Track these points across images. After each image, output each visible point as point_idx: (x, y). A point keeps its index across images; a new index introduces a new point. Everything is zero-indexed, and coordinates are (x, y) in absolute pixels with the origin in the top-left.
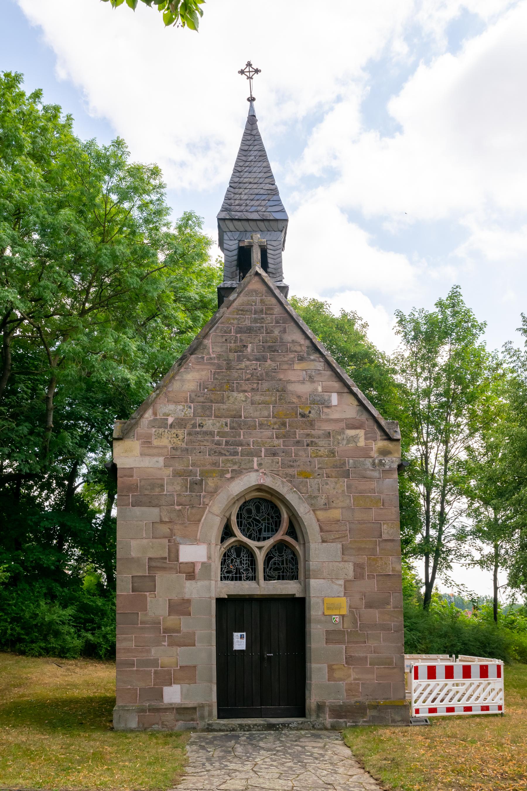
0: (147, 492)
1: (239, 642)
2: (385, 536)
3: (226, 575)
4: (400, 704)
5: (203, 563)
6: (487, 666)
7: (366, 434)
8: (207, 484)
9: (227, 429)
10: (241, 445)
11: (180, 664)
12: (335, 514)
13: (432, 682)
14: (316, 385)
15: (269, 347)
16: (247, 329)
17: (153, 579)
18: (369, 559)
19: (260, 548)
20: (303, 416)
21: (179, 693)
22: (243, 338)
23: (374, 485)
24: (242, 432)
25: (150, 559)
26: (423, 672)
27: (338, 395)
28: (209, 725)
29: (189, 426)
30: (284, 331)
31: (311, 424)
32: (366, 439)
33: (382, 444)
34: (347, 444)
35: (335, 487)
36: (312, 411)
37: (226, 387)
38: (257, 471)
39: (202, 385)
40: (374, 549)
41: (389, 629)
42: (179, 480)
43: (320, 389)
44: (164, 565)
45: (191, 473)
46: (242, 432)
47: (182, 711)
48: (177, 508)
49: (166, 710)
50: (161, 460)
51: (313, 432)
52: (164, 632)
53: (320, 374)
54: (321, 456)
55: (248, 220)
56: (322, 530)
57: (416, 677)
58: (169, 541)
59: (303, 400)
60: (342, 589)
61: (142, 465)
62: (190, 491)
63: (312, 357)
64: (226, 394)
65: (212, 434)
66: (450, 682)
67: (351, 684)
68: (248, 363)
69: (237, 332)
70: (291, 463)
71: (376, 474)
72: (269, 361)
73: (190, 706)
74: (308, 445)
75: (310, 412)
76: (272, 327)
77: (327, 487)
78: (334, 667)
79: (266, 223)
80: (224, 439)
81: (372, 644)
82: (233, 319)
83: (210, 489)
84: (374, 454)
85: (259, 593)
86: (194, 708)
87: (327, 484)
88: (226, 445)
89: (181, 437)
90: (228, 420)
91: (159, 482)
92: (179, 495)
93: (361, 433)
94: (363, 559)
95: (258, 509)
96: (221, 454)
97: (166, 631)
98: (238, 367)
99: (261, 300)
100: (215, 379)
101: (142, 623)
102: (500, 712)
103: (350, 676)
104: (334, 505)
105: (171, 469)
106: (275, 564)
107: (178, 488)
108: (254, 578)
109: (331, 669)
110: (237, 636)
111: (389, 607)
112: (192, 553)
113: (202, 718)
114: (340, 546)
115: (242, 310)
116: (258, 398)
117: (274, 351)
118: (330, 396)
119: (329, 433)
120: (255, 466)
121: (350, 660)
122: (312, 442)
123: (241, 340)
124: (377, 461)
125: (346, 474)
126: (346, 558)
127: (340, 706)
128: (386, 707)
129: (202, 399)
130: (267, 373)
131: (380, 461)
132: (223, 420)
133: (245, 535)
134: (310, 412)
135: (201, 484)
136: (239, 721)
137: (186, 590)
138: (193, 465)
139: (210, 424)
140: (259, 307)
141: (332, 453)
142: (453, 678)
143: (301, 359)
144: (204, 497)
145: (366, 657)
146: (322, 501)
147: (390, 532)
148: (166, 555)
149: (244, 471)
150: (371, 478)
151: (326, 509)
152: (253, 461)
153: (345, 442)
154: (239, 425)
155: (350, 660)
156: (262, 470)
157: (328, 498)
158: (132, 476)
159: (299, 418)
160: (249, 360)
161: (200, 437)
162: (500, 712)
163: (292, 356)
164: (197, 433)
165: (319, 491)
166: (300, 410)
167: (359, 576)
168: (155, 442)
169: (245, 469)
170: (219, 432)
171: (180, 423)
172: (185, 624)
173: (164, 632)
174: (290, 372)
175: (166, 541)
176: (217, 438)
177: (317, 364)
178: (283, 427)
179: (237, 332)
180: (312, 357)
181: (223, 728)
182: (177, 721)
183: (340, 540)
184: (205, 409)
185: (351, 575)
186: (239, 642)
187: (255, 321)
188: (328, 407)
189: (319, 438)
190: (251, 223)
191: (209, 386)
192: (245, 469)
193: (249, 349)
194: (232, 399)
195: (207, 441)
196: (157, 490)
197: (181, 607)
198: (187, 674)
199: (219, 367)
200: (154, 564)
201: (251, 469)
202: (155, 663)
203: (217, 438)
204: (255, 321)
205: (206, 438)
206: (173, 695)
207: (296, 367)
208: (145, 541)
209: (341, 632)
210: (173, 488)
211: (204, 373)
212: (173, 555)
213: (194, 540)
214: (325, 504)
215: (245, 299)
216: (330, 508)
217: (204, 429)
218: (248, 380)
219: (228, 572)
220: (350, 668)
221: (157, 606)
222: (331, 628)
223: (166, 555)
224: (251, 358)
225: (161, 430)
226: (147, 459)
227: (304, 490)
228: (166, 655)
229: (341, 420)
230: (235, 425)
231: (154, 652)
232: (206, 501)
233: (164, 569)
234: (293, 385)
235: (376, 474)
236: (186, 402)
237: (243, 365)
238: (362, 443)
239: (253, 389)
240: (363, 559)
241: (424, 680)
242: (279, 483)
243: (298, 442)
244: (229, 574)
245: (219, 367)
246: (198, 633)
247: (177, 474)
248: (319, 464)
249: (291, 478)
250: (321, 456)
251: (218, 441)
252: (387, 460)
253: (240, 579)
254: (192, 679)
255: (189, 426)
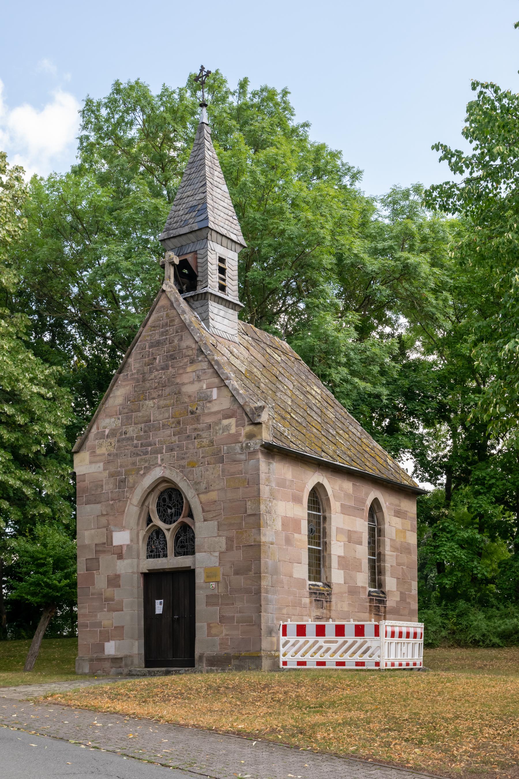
0: (93, 492)
1: (159, 608)
2: (249, 512)
3: (150, 554)
4: (256, 655)
5: (128, 545)
6: (363, 626)
7: (237, 422)
8: (128, 481)
9: (142, 433)
10: (150, 445)
11: (114, 625)
12: (213, 495)
13: (302, 639)
14: (202, 383)
15: (171, 355)
16: (157, 343)
17: (97, 559)
18: (237, 532)
19: (168, 530)
20: (192, 413)
21: (114, 647)
22: (154, 352)
23: (241, 467)
24: (151, 433)
25: (96, 545)
26: (292, 629)
27: (218, 389)
28: (130, 671)
29: (118, 434)
30: (181, 339)
31: (198, 419)
32: (237, 426)
33: (248, 428)
34: (223, 433)
35: (212, 473)
36: (199, 408)
37: (141, 397)
38: (160, 465)
39: (127, 399)
40: (241, 523)
41: (251, 592)
42: (112, 479)
43: (205, 387)
44: (105, 549)
45: (119, 473)
46: (151, 433)
47: (115, 660)
48: (111, 502)
49: (105, 659)
50: (101, 464)
51: (199, 426)
52: (105, 601)
53: (205, 372)
54: (204, 447)
55: (180, 235)
56: (204, 511)
57: (285, 634)
58: (107, 530)
59: (192, 398)
60: (218, 560)
61: (91, 471)
62: (119, 488)
63: (200, 359)
64: (141, 403)
65: (131, 439)
66: (321, 639)
67: (223, 639)
68: (156, 373)
69: (150, 348)
70: (183, 456)
71: (243, 457)
72: (170, 368)
73: (119, 656)
74: (195, 438)
75: (197, 409)
76: (173, 337)
77: (208, 473)
78: (211, 625)
79: (194, 233)
80: (140, 442)
81: (239, 605)
82: (148, 336)
83: (131, 485)
84: (242, 439)
85: (167, 567)
86: (121, 658)
87: (207, 470)
88: (141, 447)
89: (113, 445)
90: (143, 425)
91: (100, 483)
92: (112, 492)
93: (233, 421)
94: (233, 533)
95: (170, 497)
96: (138, 455)
97: (106, 600)
98: (150, 378)
99: (167, 314)
100: (135, 391)
101: (92, 594)
102: (377, 668)
103: (222, 632)
104: (212, 488)
105: (107, 471)
106: (181, 542)
107: (111, 486)
108: (165, 556)
109: (209, 627)
110: (158, 602)
111: (251, 573)
112: (121, 538)
113: (126, 665)
114: (216, 523)
115: (154, 327)
116: (162, 403)
117: (173, 359)
118: (212, 392)
119: (210, 425)
120: (159, 462)
121: (223, 619)
122: (198, 435)
123: (153, 354)
124: (244, 445)
125: (221, 460)
126: (220, 533)
127: (214, 657)
128: (245, 658)
129: (126, 411)
130: (168, 380)
131: (247, 444)
132: (139, 426)
133: (161, 520)
134: (197, 409)
135: (125, 482)
136: (157, 669)
137: (117, 568)
138: (121, 466)
139: (132, 431)
140: (165, 320)
141: (212, 442)
142: (324, 636)
143: (192, 362)
144: (127, 492)
145: (234, 617)
146: (203, 486)
147: (253, 508)
148: (105, 541)
149: (152, 467)
150: (239, 461)
151: (206, 493)
152: (157, 457)
153: (221, 431)
154: (149, 428)
155: (223, 619)
156: (164, 465)
157: (208, 483)
158: (85, 481)
159: (190, 416)
160: (157, 370)
161: (125, 443)
162: (377, 668)
163: (186, 360)
164: (123, 439)
165: (202, 476)
166: (190, 408)
167: (229, 548)
168: (98, 452)
169: (153, 465)
170: (137, 436)
171: (113, 433)
172: (117, 594)
173: (105, 601)
174: (184, 376)
175: (105, 529)
176: (135, 442)
177: (203, 364)
178: (178, 425)
179: (150, 348)
180: (200, 359)
181: (139, 673)
182: (112, 668)
183: (217, 518)
185: (224, 546)
186: (159, 608)
187: (162, 334)
188: (210, 402)
189: (203, 430)
190: (184, 237)
191: (131, 399)
192: (153, 465)
193: (157, 361)
194: (145, 407)
195: (129, 445)
196: (99, 490)
197: (114, 581)
198: (118, 632)
199: (138, 381)
200: (98, 549)
201: (156, 465)
202: (99, 624)
203: (135, 442)
204: (162, 334)
205: (129, 443)
206: (111, 648)
207: (189, 369)
208: (93, 531)
209: (216, 596)
210: (108, 487)
211: (128, 388)
212: (109, 541)
213: (122, 528)
214: (206, 488)
215: (156, 315)
216: (209, 491)
217: (127, 436)
218: (156, 388)
219: (151, 552)
220: (222, 626)
221: (100, 582)
222: (210, 593)
223: (105, 541)
224: (158, 368)
225: (102, 440)
226: (93, 465)
227: (191, 477)
228: (107, 619)
229: (218, 412)
230: (147, 429)
231: (100, 616)
232: (128, 494)
233: (104, 552)
234: (186, 386)
235: (243, 457)
236: (117, 415)
237: (152, 376)
238: (233, 430)
239: (159, 395)
240: (233, 533)
241: (292, 637)
242: (175, 474)
243: (188, 436)
244: (152, 554)
245: (138, 381)
246: (125, 600)
247: (111, 475)
248: (202, 453)
249: (182, 468)
250: (204, 447)
251: (136, 444)
252: (252, 443)
253: (159, 557)
254: (121, 637)
255: (118, 434)
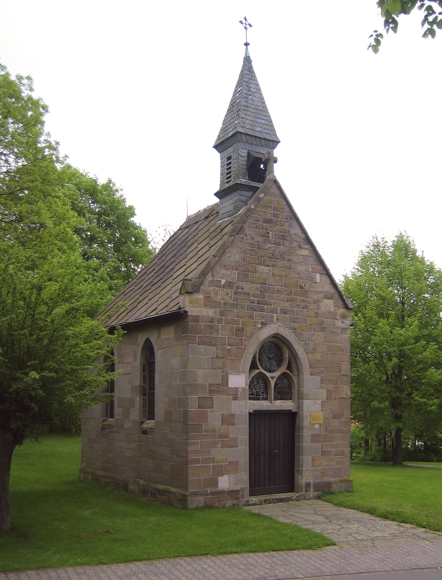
5: (243, 388)
10: (266, 304)
15: (283, 236)
18: (335, 387)
19: (272, 378)
22: (267, 227)
29: (235, 288)
36: (307, 285)
48: (229, 347)
51: (306, 299)
55: (256, 137)
58: (222, 372)
78: (315, 458)
79: (267, 142)
86: (238, 491)
89: (230, 295)
96: (255, 310)
98: (264, 248)
106: (279, 389)
109: (314, 460)
114: (320, 378)
117: (284, 239)
121: (323, 453)
122: (306, 306)
123: (266, 229)
132: (255, 285)
135: (243, 331)
148: (220, 382)
154: (265, 290)
155: (323, 453)
156: (278, 323)
160: (270, 243)
161: (241, 296)
167: (329, 398)
169: (269, 322)
175: (220, 371)
184: (245, 276)
190: (257, 140)
197: (228, 419)
198: (232, 467)
202: (213, 460)
206: (224, 483)
209: (319, 435)
214: (313, 350)
216: (315, 352)
223: (220, 382)
224: (272, 242)
228: (220, 454)
230: (262, 289)
233: (218, 392)
239: (273, 265)
240: (331, 387)
255: (235, 288)
